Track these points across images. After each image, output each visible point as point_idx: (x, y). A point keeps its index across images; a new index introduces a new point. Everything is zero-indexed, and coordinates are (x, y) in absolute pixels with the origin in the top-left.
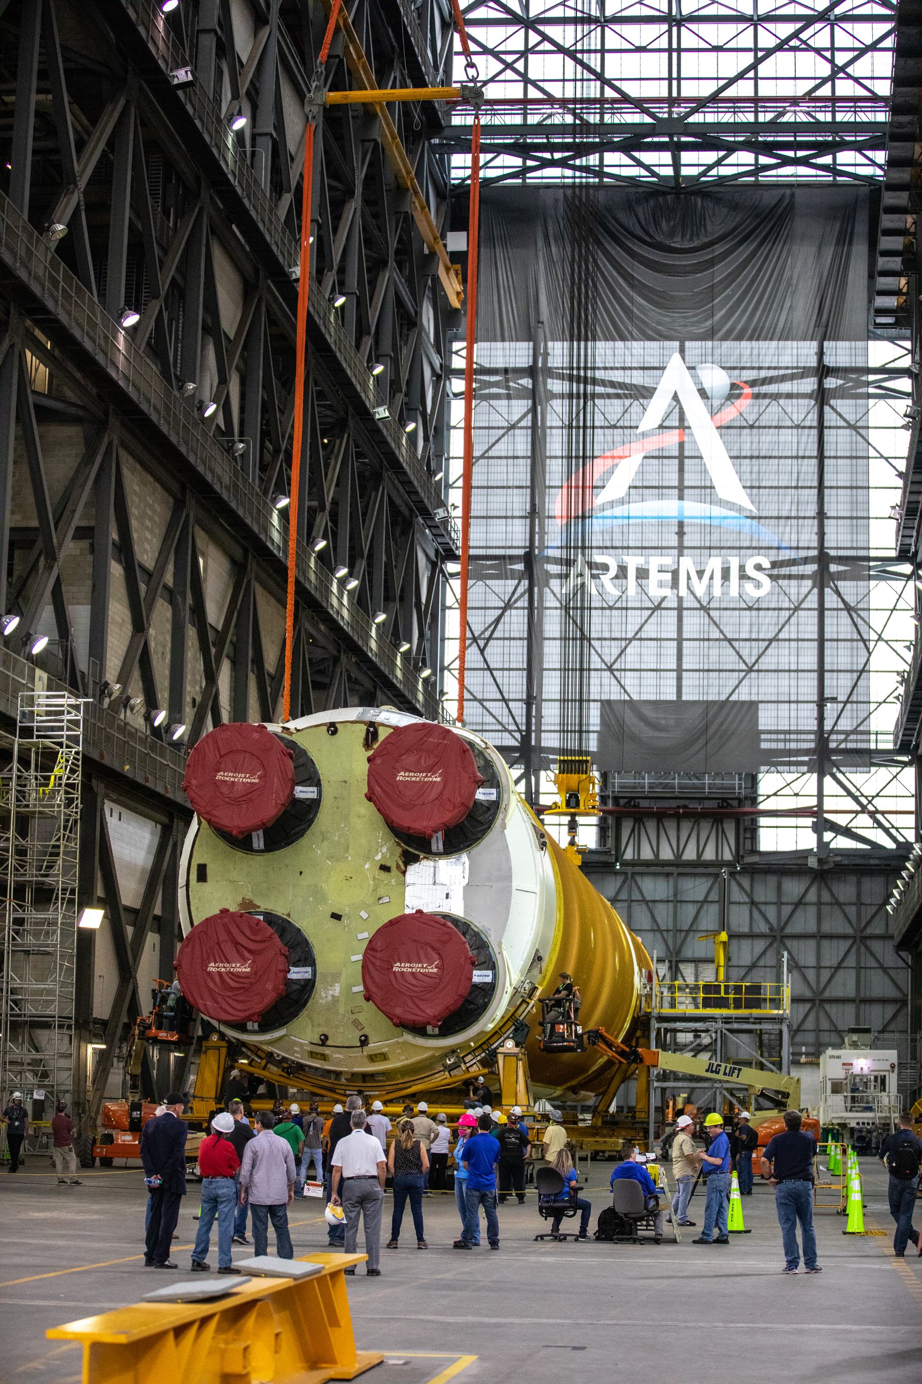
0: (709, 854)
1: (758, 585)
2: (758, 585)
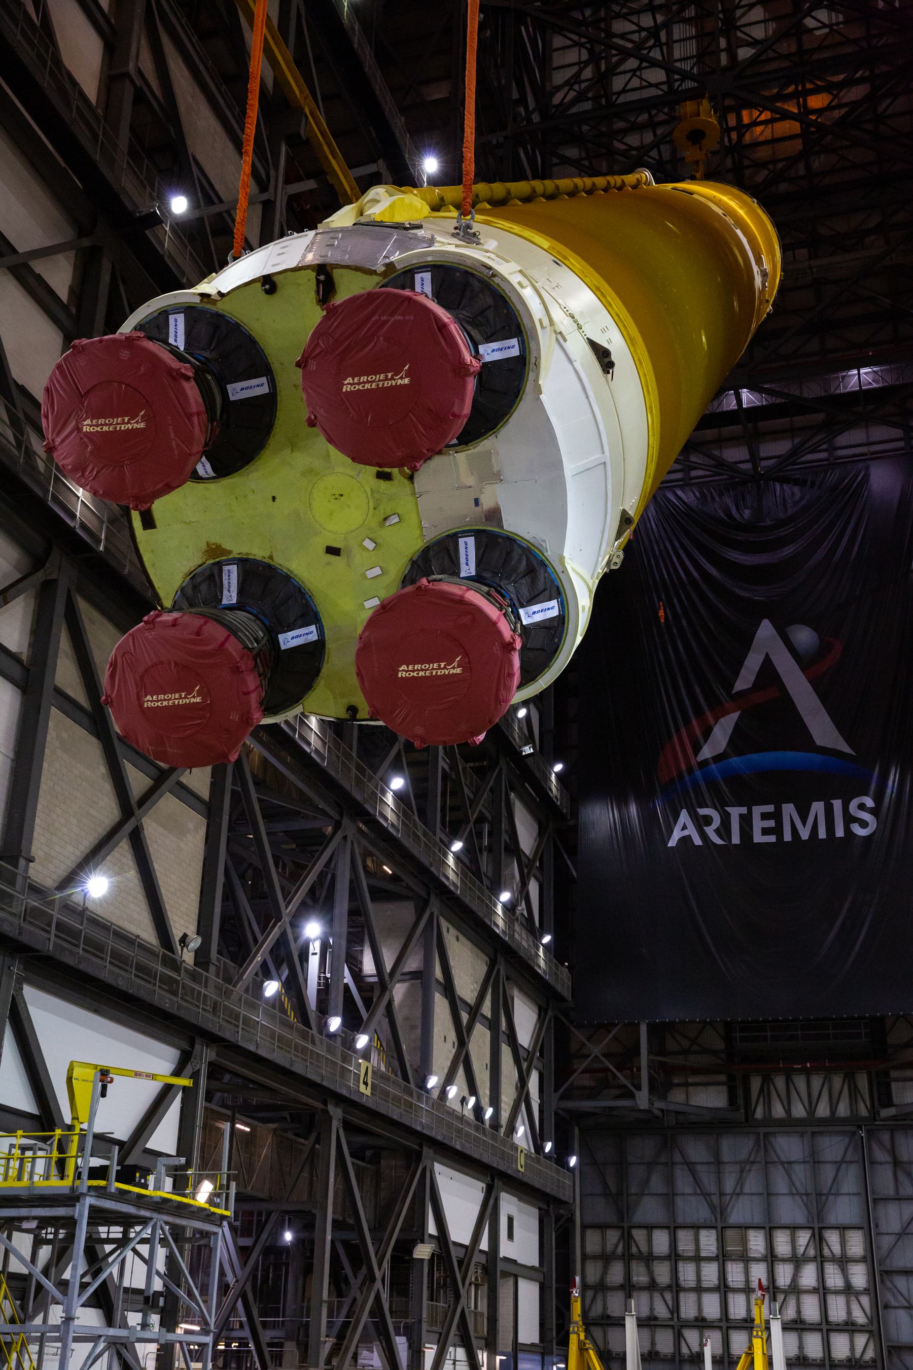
1: (864, 824)
2: (864, 824)
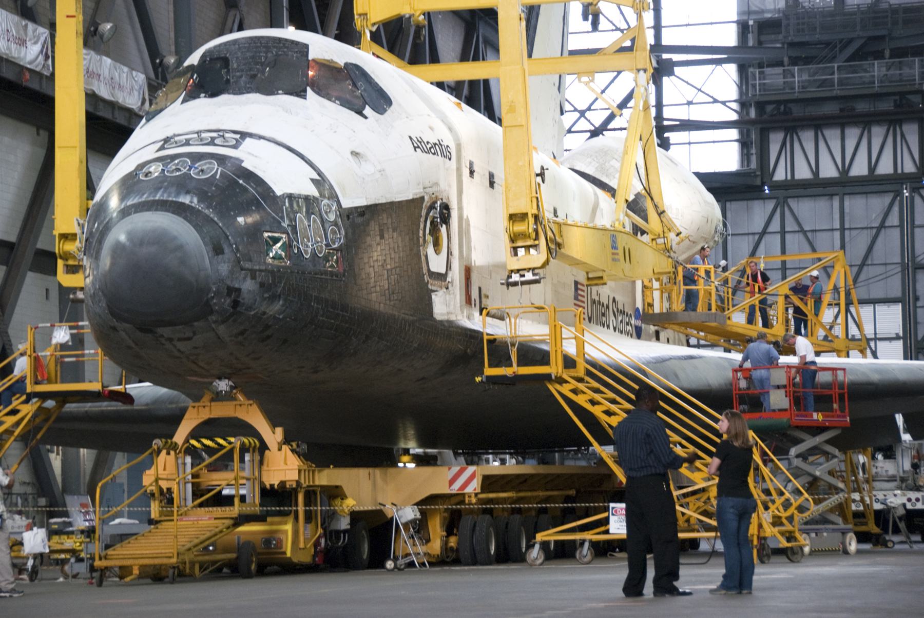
0: (885, 167)
